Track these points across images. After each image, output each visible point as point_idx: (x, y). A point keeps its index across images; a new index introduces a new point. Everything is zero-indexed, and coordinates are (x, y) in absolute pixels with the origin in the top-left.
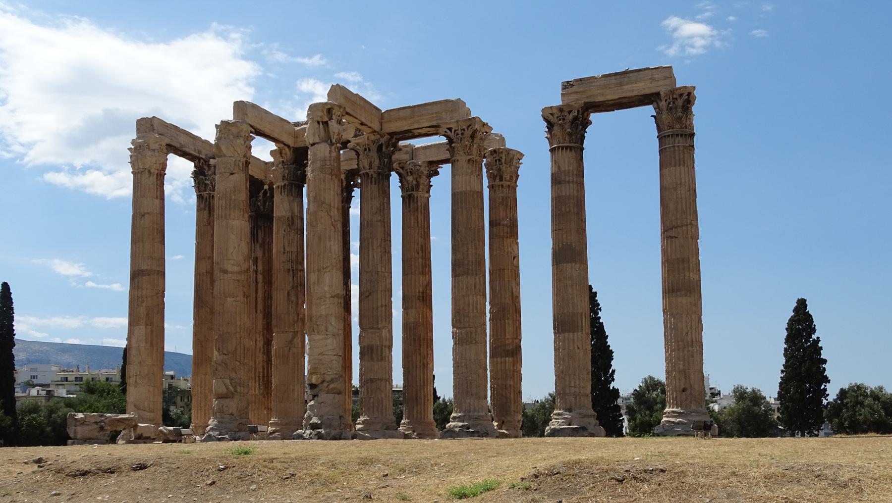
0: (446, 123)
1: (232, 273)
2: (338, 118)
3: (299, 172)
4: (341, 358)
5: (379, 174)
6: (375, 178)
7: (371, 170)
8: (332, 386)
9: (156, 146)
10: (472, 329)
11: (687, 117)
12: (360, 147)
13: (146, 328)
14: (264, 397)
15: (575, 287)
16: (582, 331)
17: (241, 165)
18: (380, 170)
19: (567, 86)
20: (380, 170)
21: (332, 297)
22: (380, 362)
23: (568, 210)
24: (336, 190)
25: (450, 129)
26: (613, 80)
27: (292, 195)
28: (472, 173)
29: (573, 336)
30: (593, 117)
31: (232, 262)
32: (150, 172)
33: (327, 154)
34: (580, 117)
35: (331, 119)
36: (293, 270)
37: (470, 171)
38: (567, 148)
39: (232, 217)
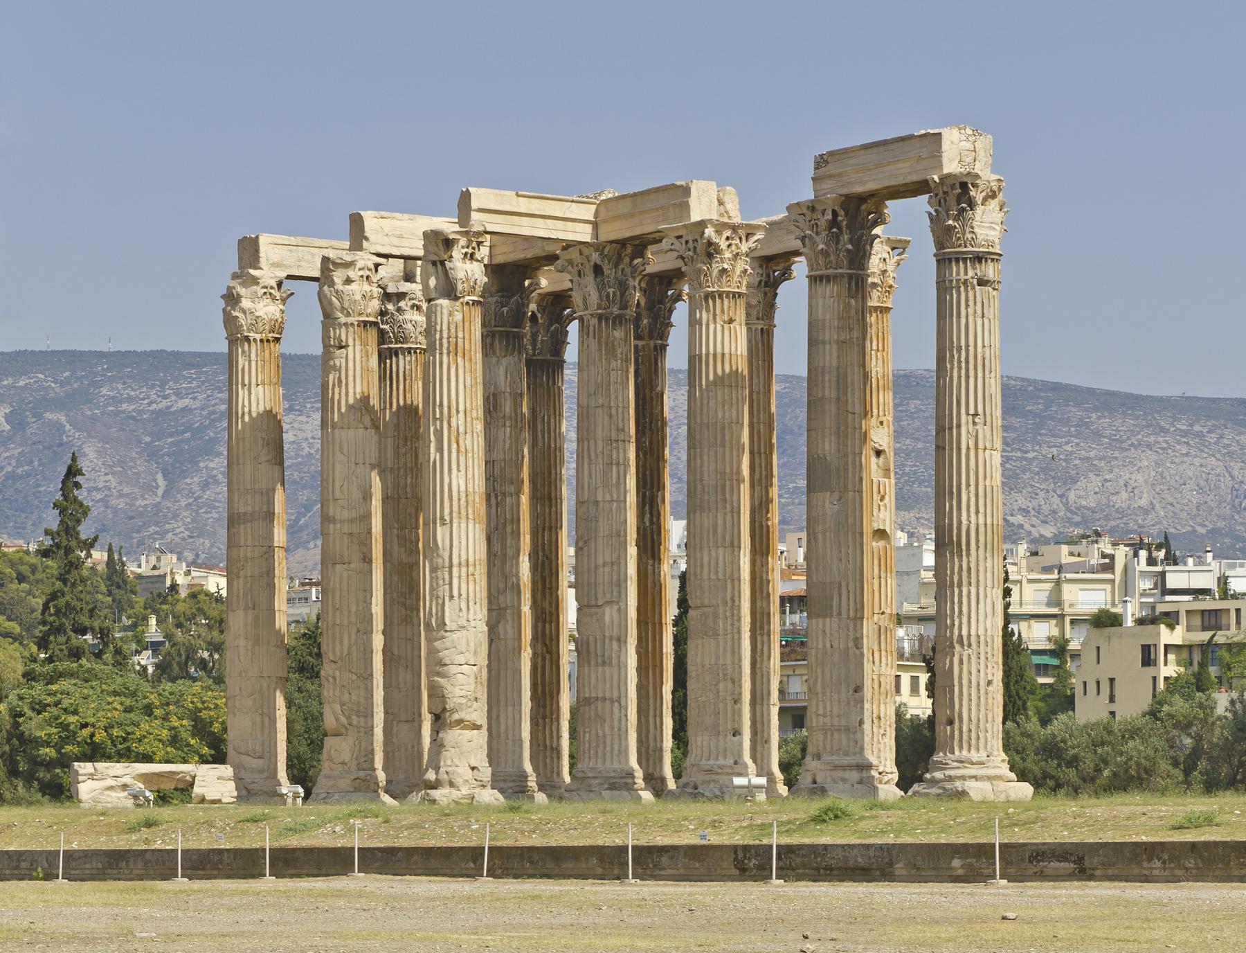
2: (466, 250)
3: (505, 309)
4: (475, 668)
5: (600, 317)
6: (594, 327)
7: (586, 312)
10: (706, 610)
12: (572, 267)
13: (246, 615)
15: (828, 534)
16: (840, 614)
18: (600, 311)
19: (821, 162)
20: (600, 311)
22: (600, 669)
23: (820, 395)
29: (824, 625)
30: (893, 207)
34: (842, 221)
36: (496, 497)
38: (821, 278)
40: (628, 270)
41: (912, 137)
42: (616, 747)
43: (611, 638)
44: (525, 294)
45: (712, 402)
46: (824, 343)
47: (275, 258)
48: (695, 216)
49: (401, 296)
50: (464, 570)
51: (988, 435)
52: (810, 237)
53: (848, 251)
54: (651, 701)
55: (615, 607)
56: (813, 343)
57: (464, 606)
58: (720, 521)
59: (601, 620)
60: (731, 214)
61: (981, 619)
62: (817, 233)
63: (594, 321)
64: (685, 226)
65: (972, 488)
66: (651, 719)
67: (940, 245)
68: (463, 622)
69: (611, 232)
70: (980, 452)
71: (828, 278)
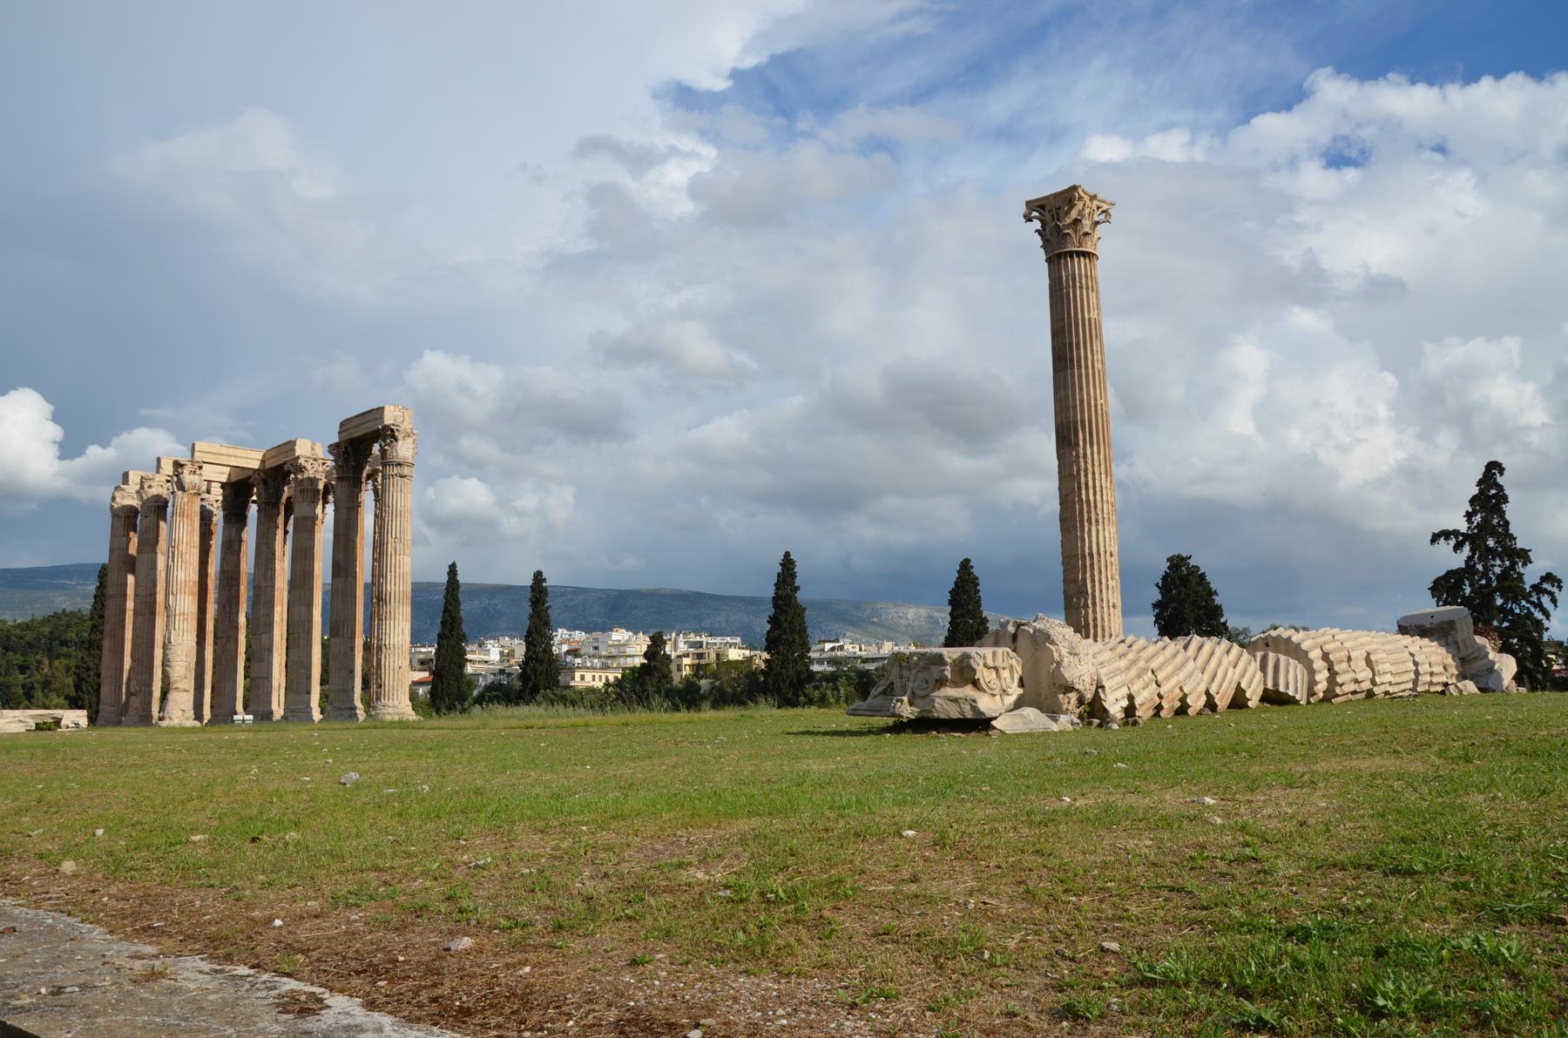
1: (142, 596)
5: (265, 503)
8: (174, 686)
11: (392, 448)
16: (343, 635)
19: (342, 424)
25: (292, 465)
28: (303, 501)
32: (118, 515)
40: (281, 483)
43: (265, 649)
48: (297, 455)
50: (182, 617)
51: (402, 548)
55: (267, 635)
57: (181, 634)
59: (260, 641)
61: (396, 636)
64: (293, 459)
65: (393, 574)
68: (180, 641)
69: (269, 465)
70: (398, 557)
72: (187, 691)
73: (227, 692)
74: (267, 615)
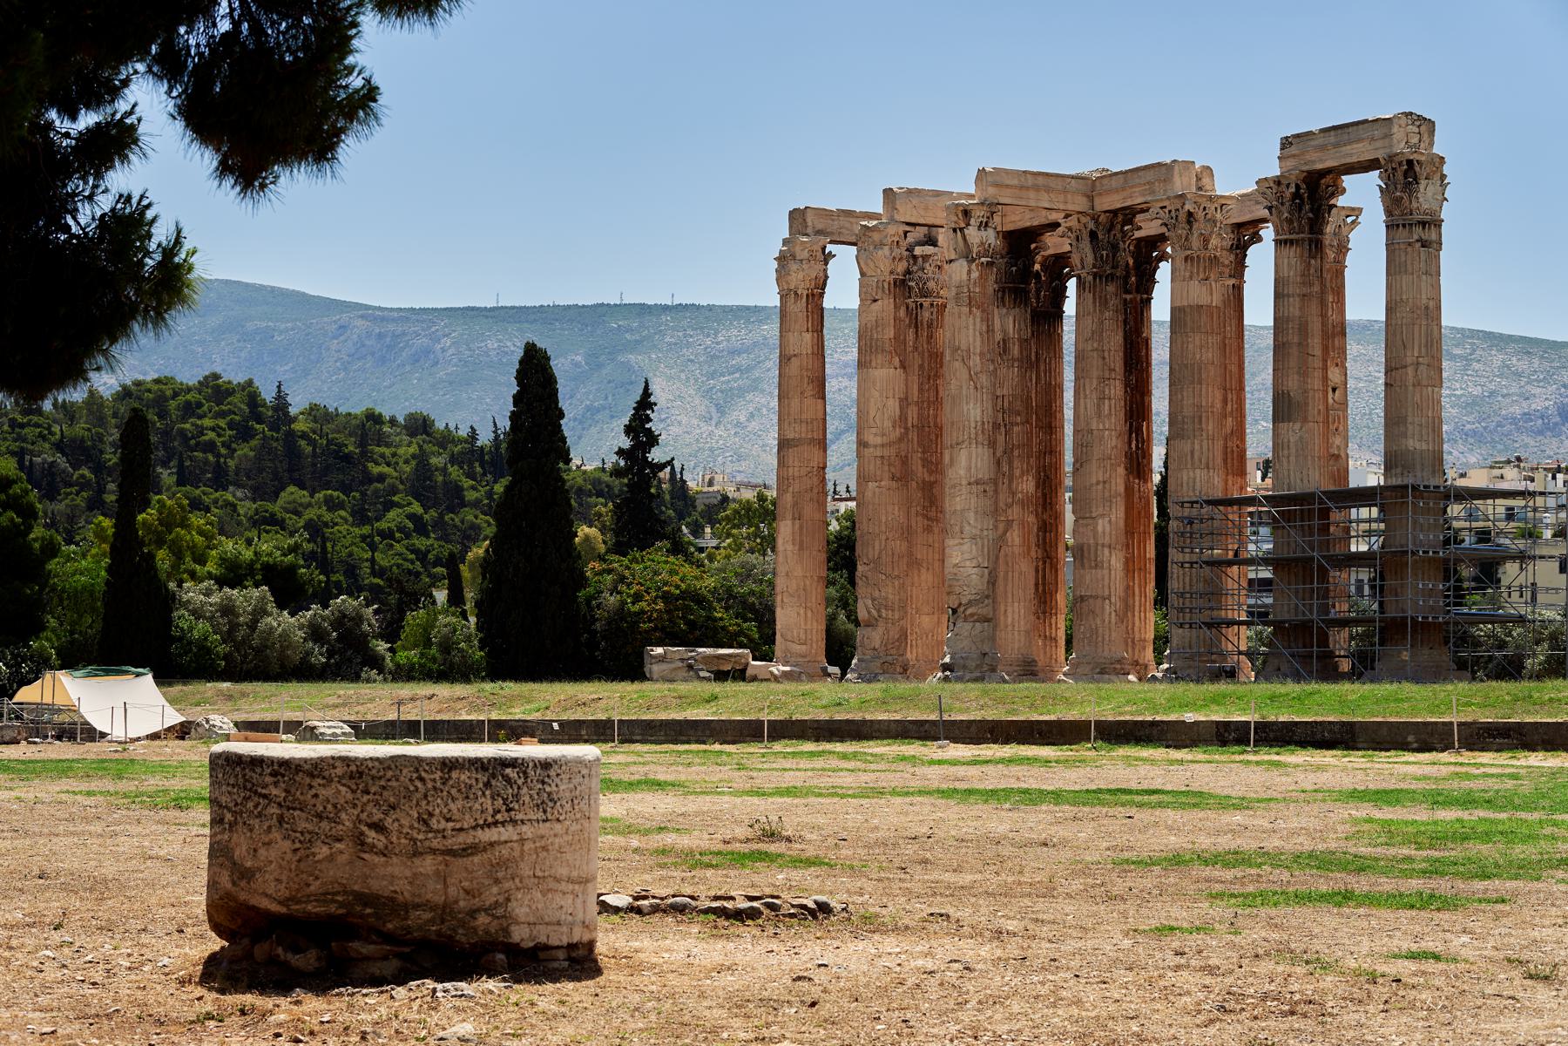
0: (1157, 201)
1: (875, 446)
3: (1014, 269)
5: (1095, 275)
8: (968, 612)
9: (805, 254)
14: (1038, 618)
17: (886, 286)
19: (1286, 143)
21: (969, 484)
24: (978, 327)
26: (1332, 138)
27: (1004, 306)
28: (1191, 278)
30: (1348, 181)
31: (874, 430)
32: (796, 293)
33: (965, 277)
35: (968, 224)
37: (1188, 274)
38: (1286, 241)
39: (874, 364)
40: (1119, 236)
41: (1366, 121)
42: (1107, 637)
43: (1103, 546)
44: (1030, 257)
45: (1191, 346)
46: (1288, 296)
47: (820, 226)
49: (925, 258)
52: (1277, 207)
53: (1309, 219)
54: (1137, 598)
56: (1278, 296)
58: (1197, 447)
59: (1095, 531)
60: (1208, 187)
62: (1282, 204)
63: (1090, 278)
66: (1137, 614)
67: (1388, 212)
71: (1292, 242)
72: (988, 620)
73: (1010, 620)
74: (1104, 482)
